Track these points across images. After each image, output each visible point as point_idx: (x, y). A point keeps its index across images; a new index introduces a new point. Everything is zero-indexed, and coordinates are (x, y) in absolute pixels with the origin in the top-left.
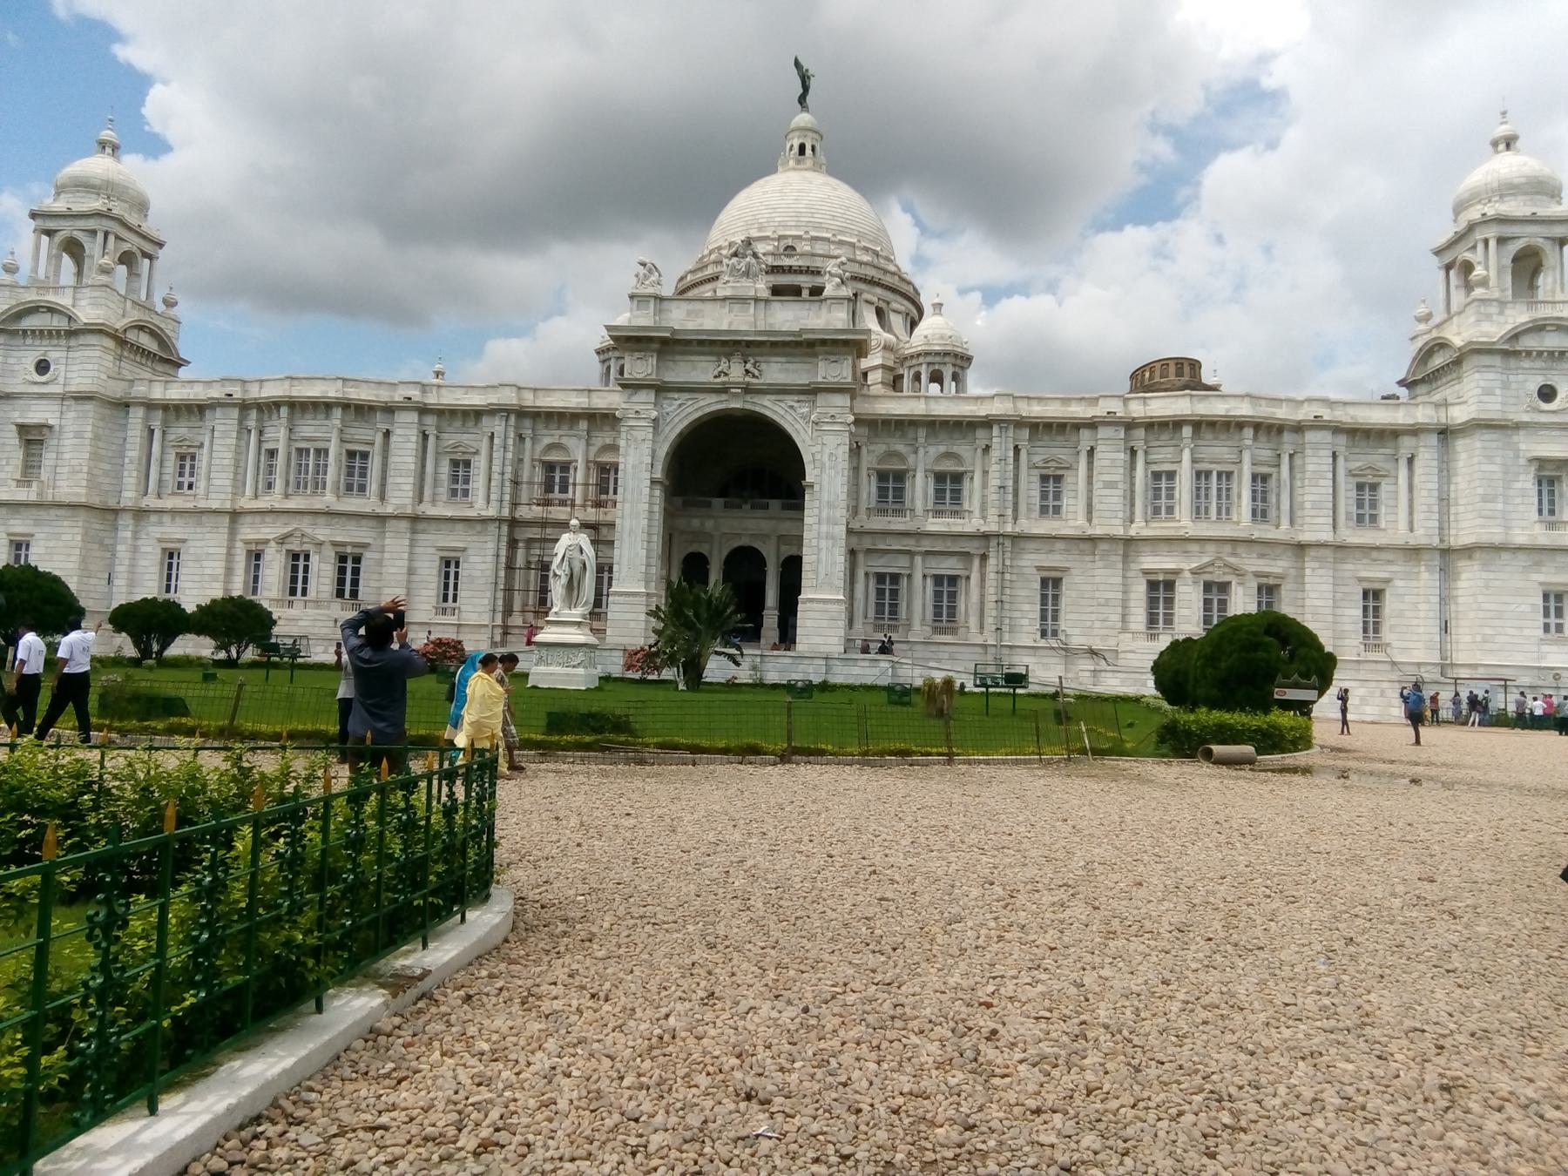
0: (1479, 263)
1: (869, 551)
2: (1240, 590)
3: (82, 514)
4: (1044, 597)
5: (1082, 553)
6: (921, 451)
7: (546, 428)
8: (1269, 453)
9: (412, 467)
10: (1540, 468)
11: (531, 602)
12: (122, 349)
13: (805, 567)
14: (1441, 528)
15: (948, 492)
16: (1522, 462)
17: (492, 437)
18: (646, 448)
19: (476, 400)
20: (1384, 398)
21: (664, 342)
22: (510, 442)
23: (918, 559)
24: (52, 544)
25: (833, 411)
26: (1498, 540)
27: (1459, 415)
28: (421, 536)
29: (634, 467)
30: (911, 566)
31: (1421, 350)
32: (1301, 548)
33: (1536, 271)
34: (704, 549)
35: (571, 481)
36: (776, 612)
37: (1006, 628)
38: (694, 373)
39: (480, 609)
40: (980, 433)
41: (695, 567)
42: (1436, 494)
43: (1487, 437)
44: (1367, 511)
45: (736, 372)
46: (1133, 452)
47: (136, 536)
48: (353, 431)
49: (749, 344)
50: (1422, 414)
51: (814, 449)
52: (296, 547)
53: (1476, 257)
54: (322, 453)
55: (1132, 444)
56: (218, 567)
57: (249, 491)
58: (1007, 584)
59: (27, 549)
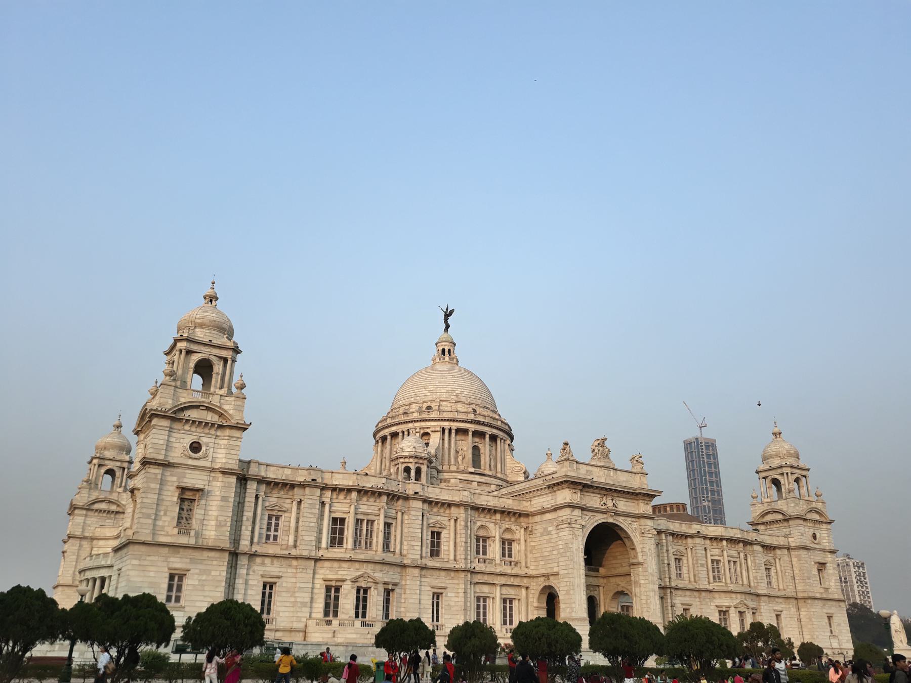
3: (226, 555)
7: (479, 516)
16: (813, 563)
17: (456, 521)
18: (580, 539)
24: (204, 578)
25: (649, 528)
28: (423, 579)
31: (763, 511)
32: (758, 595)
38: (591, 503)
45: (610, 504)
49: (616, 490)
50: (782, 541)
54: (371, 522)
55: (706, 546)
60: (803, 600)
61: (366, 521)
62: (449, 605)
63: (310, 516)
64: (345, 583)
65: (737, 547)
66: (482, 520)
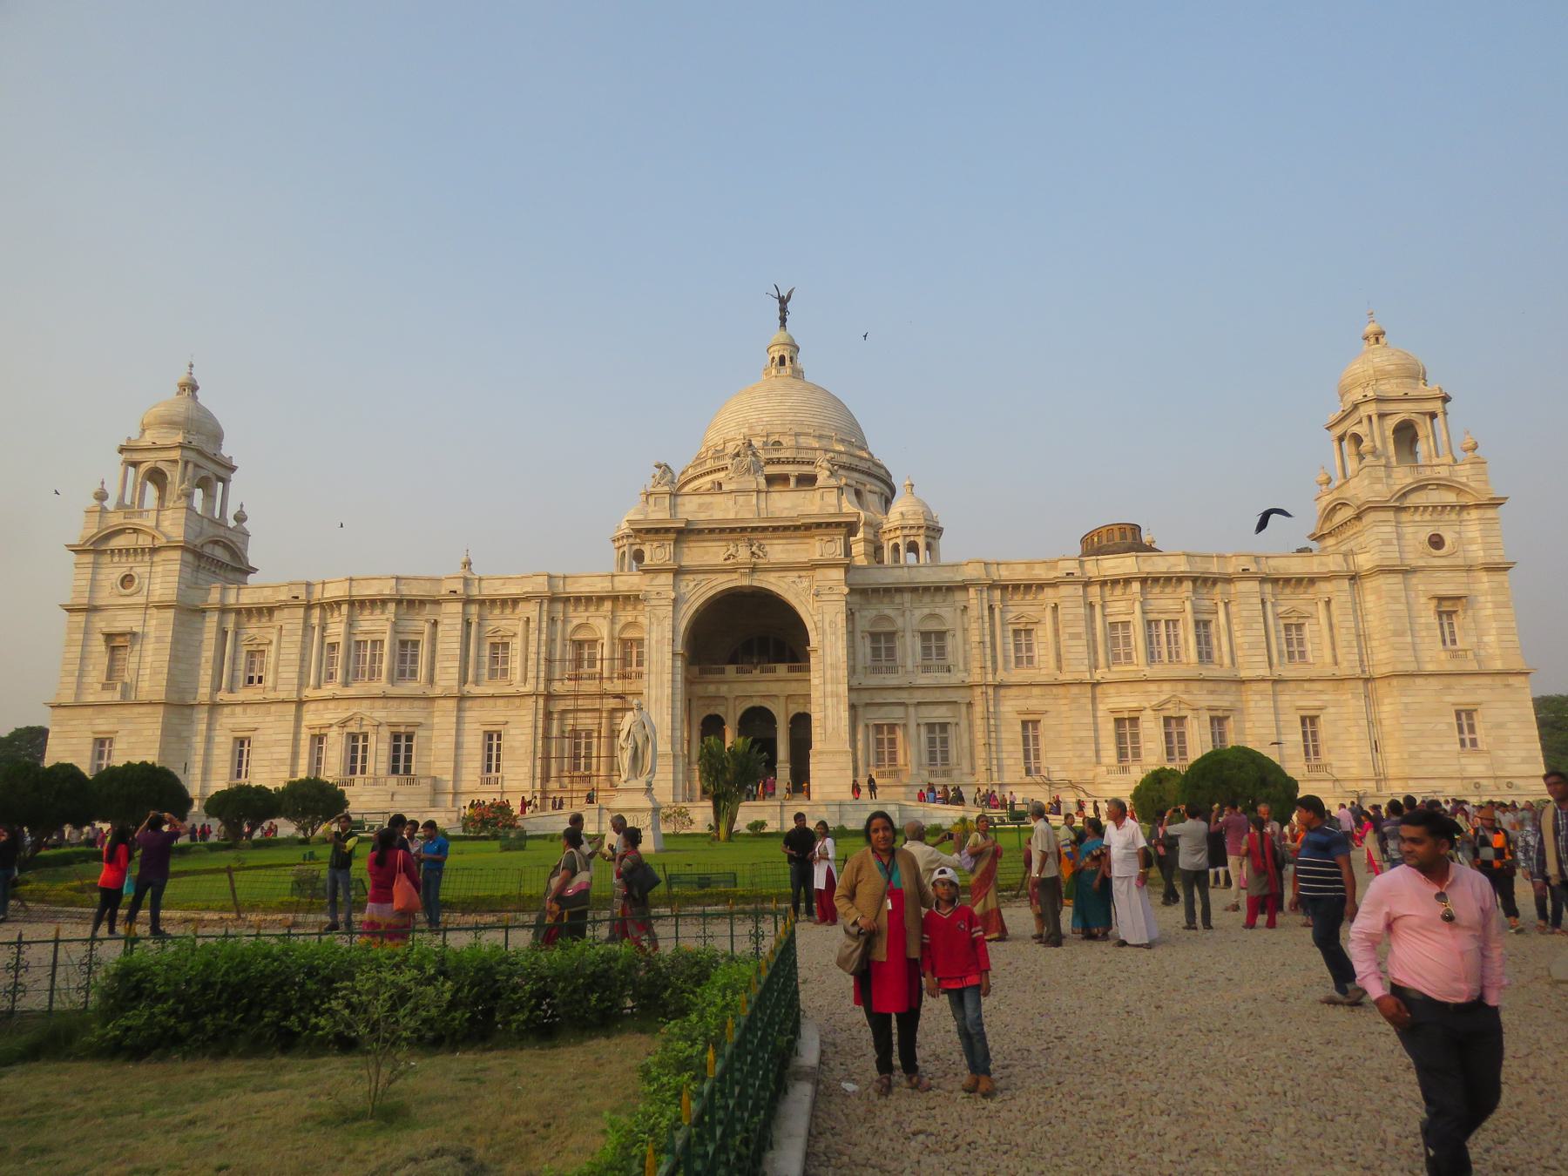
0: (1366, 436)
1: (867, 705)
2: (1195, 723)
3: (161, 709)
4: (1025, 739)
5: (1056, 698)
6: (908, 613)
7: (575, 610)
8: (1207, 602)
9: (458, 652)
10: (1439, 605)
11: (566, 768)
12: (199, 561)
13: (814, 723)
14: (1362, 661)
15: (934, 649)
16: (1423, 600)
18: (668, 623)
19: (513, 590)
20: (1299, 551)
21: (681, 533)
22: (544, 625)
23: (912, 710)
24: (133, 739)
25: (830, 583)
26: (1412, 667)
27: (1364, 561)
28: (468, 714)
29: (656, 642)
30: (907, 716)
31: (1325, 509)
32: (1243, 682)
33: (1414, 439)
34: (720, 711)
35: (599, 657)
36: (788, 765)
37: (995, 768)
39: (522, 777)
40: (959, 596)
41: (713, 725)
42: (1353, 631)
43: (1390, 581)
44: (1295, 648)
45: (743, 554)
46: (1091, 606)
47: (210, 728)
48: (406, 623)
49: (754, 529)
50: (1333, 563)
51: (816, 618)
52: (354, 728)
53: (1360, 430)
56: (285, 752)
57: (312, 681)
58: (992, 729)
59: (111, 745)
60: (1387, 681)
61: (369, 642)
62: (511, 747)
63: (287, 645)
64: (332, 729)
65: (1179, 590)
66: (578, 616)
